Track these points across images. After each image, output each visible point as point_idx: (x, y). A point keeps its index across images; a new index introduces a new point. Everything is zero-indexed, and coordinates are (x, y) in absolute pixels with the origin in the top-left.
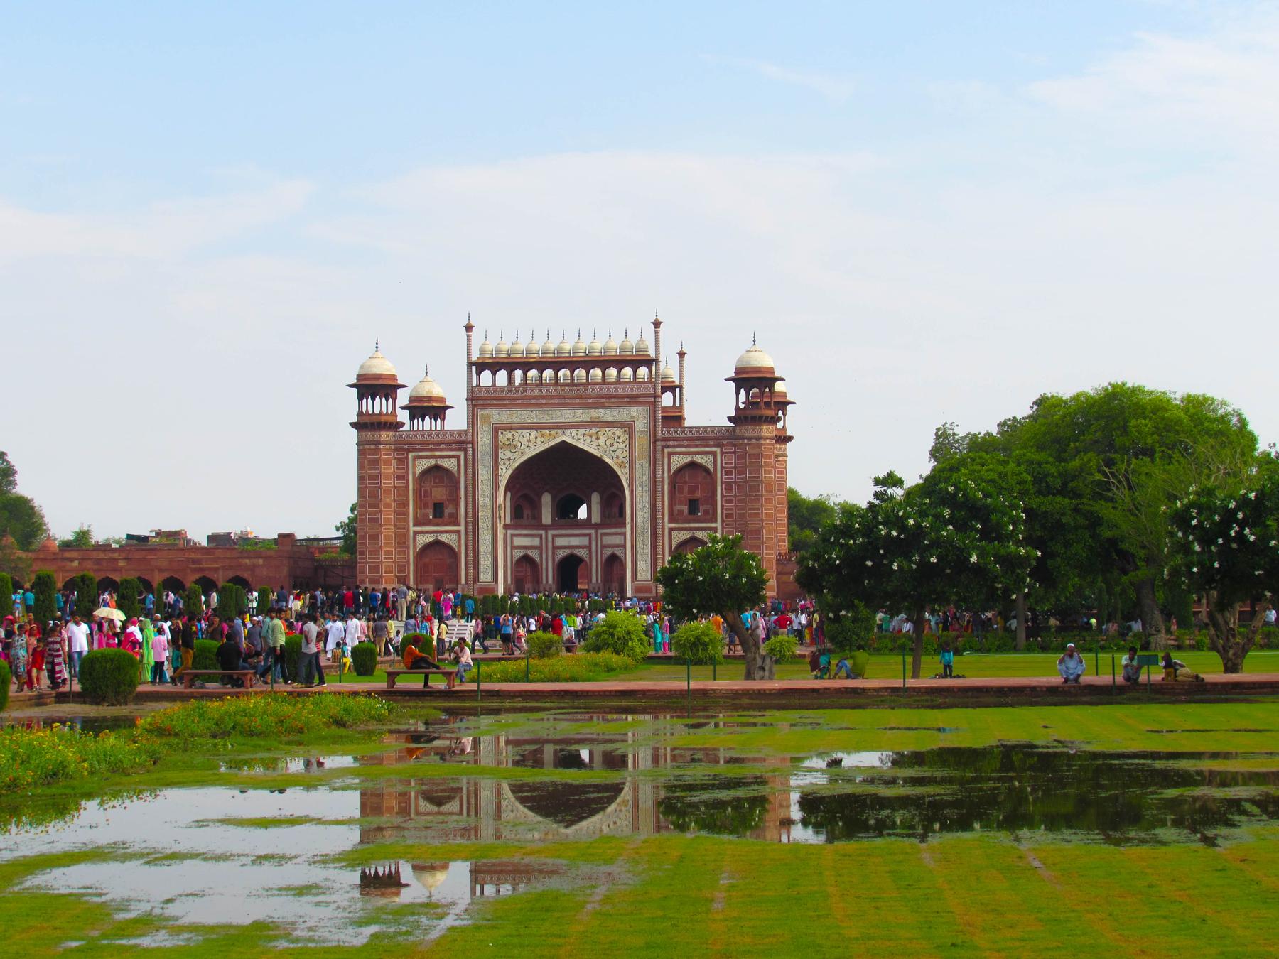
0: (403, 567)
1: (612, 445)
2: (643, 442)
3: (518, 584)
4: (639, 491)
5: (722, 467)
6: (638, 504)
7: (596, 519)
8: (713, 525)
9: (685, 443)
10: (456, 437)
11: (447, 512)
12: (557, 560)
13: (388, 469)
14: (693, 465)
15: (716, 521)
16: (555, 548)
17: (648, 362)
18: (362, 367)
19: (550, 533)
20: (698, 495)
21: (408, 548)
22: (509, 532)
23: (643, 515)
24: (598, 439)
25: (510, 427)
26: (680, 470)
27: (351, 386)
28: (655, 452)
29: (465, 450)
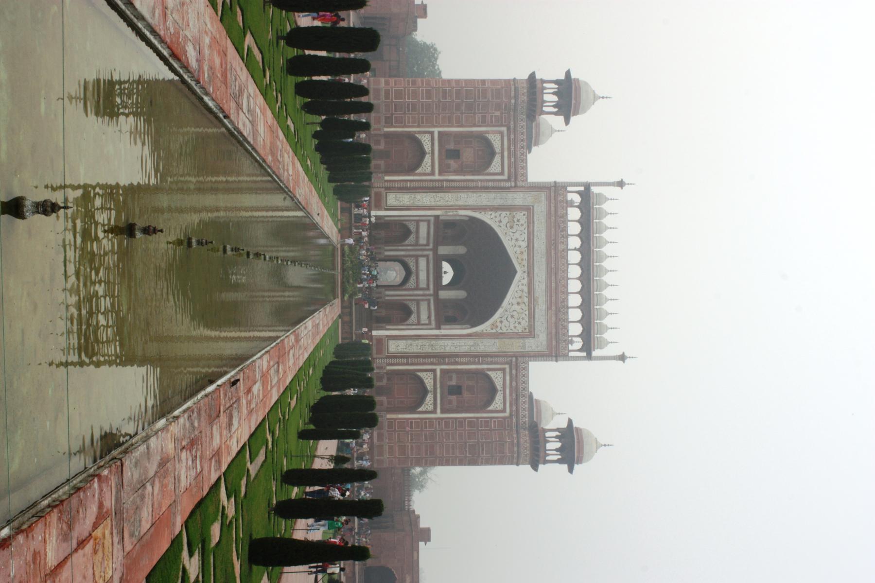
0: (401, 122)
1: (512, 316)
2: (515, 346)
3: (381, 224)
4: (470, 342)
5: (491, 418)
6: (457, 340)
7: (444, 294)
8: (439, 410)
9: (514, 384)
10: (520, 171)
11: (452, 162)
12: (406, 259)
14: (493, 391)
15: (442, 412)
16: (417, 257)
18: (586, 83)
19: (430, 253)
20: (466, 395)
21: (419, 126)
22: (432, 219)
23: (449, 346)
24: (518, 304)
25: (530, 222)
26: (488, 378)
27: (568, 73)
28: (506, 356)
29: (509, 180)
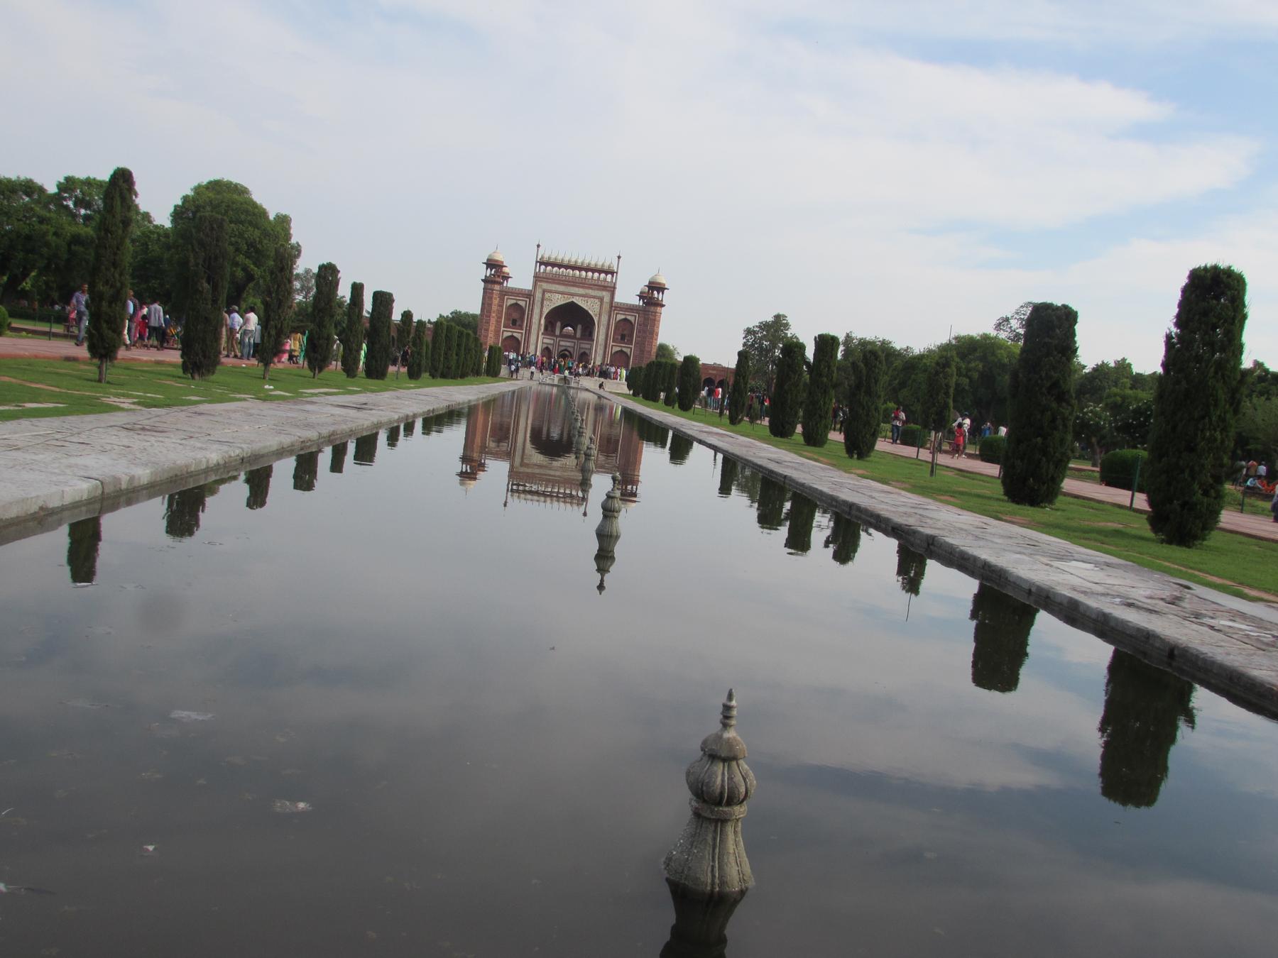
2: (606, 306)
6: (600, 334)
7: (578, 335)
13: (496, 301)
14: (625, 320)
17: (612, 273)
23: (602, 337)
25: (550, 291)
